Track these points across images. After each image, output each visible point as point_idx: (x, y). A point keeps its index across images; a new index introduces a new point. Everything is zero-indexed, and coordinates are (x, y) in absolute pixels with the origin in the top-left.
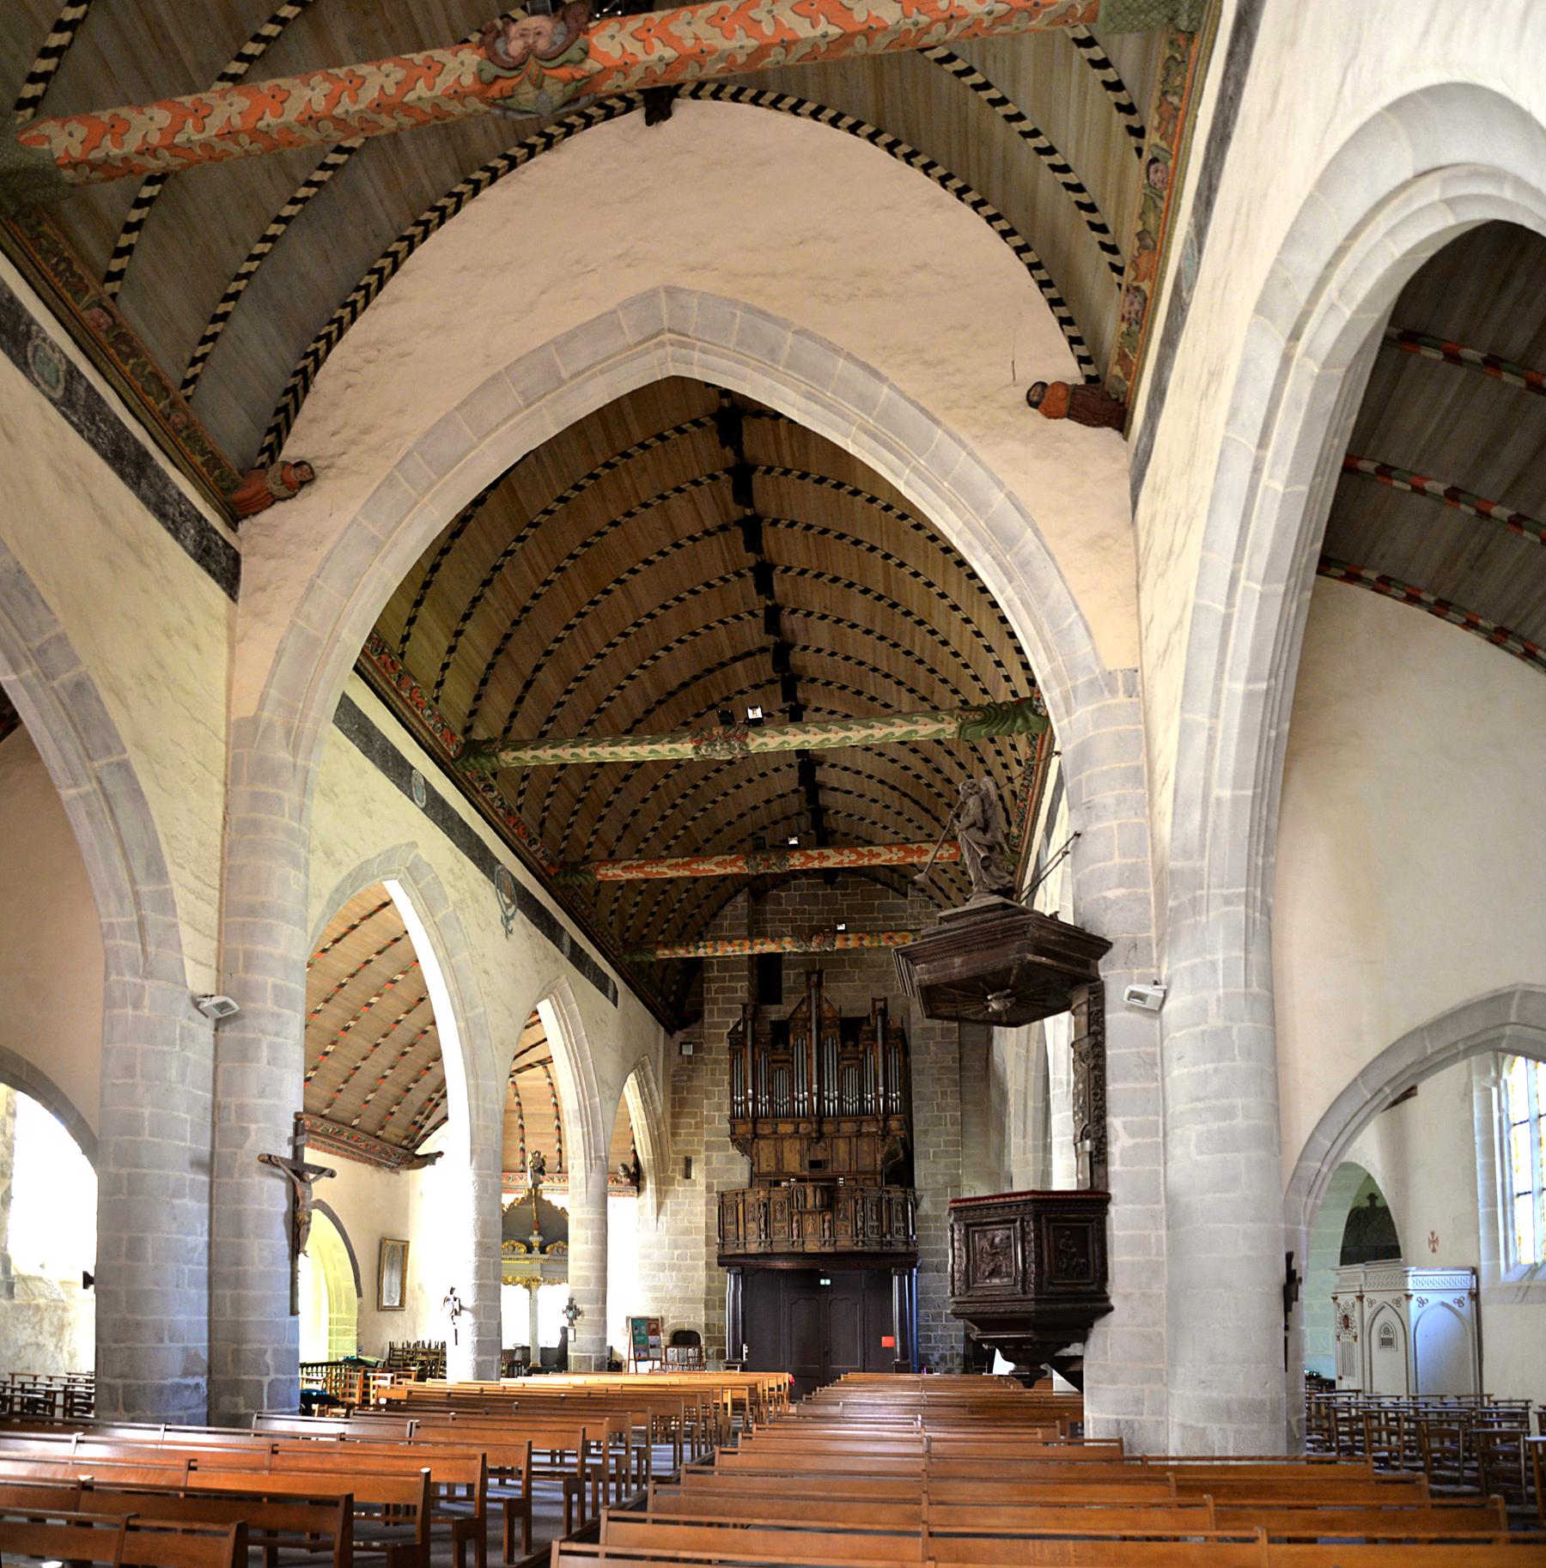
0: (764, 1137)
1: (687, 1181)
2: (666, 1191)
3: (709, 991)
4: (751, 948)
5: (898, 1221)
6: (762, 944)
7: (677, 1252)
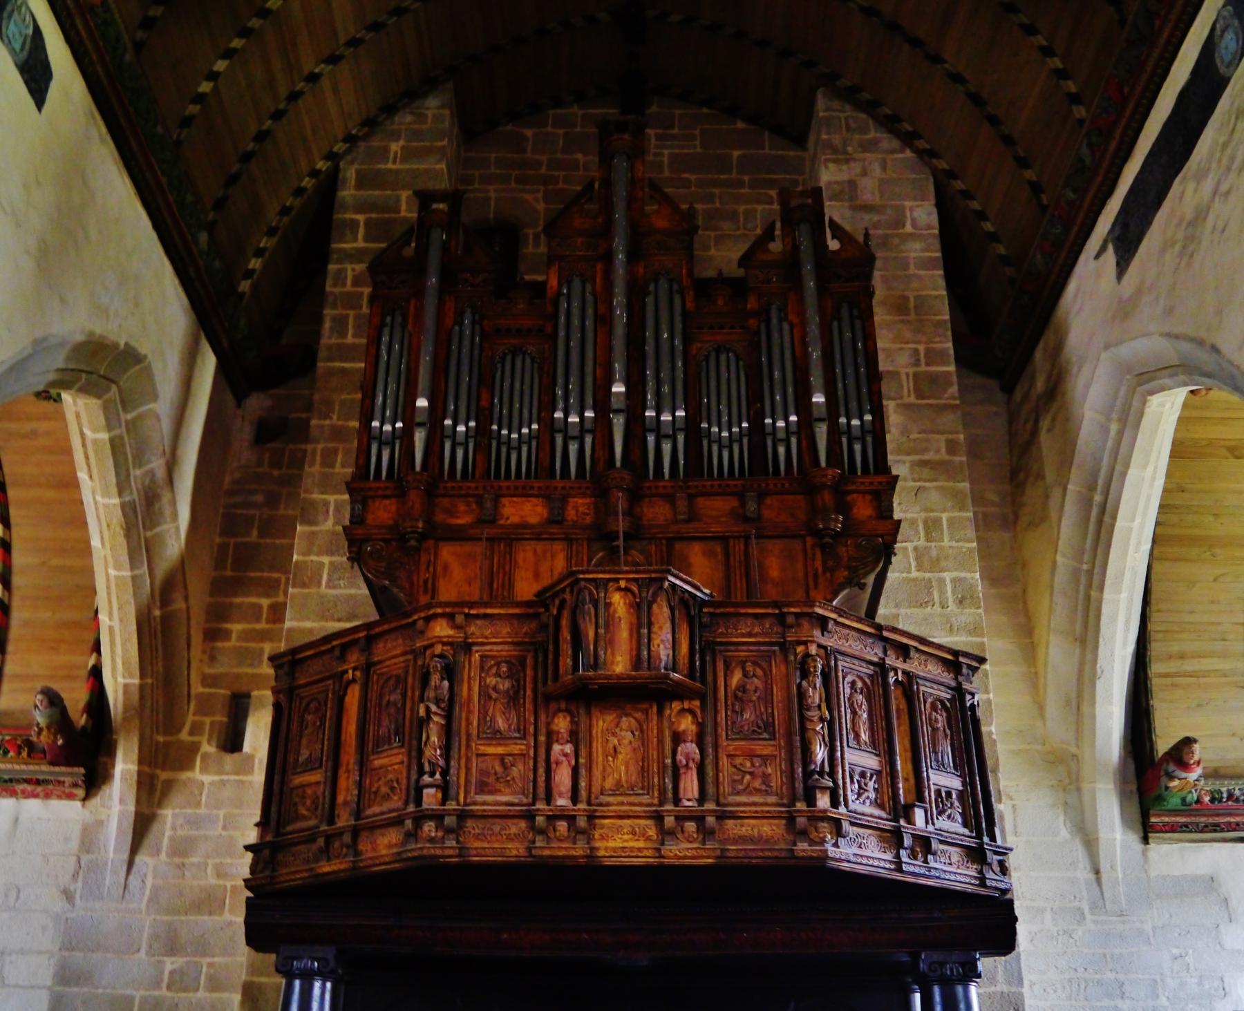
0: (457, 535)
1: (229, 759)
2: (169, 786)
5: (941, 766)
7: (170, 964)
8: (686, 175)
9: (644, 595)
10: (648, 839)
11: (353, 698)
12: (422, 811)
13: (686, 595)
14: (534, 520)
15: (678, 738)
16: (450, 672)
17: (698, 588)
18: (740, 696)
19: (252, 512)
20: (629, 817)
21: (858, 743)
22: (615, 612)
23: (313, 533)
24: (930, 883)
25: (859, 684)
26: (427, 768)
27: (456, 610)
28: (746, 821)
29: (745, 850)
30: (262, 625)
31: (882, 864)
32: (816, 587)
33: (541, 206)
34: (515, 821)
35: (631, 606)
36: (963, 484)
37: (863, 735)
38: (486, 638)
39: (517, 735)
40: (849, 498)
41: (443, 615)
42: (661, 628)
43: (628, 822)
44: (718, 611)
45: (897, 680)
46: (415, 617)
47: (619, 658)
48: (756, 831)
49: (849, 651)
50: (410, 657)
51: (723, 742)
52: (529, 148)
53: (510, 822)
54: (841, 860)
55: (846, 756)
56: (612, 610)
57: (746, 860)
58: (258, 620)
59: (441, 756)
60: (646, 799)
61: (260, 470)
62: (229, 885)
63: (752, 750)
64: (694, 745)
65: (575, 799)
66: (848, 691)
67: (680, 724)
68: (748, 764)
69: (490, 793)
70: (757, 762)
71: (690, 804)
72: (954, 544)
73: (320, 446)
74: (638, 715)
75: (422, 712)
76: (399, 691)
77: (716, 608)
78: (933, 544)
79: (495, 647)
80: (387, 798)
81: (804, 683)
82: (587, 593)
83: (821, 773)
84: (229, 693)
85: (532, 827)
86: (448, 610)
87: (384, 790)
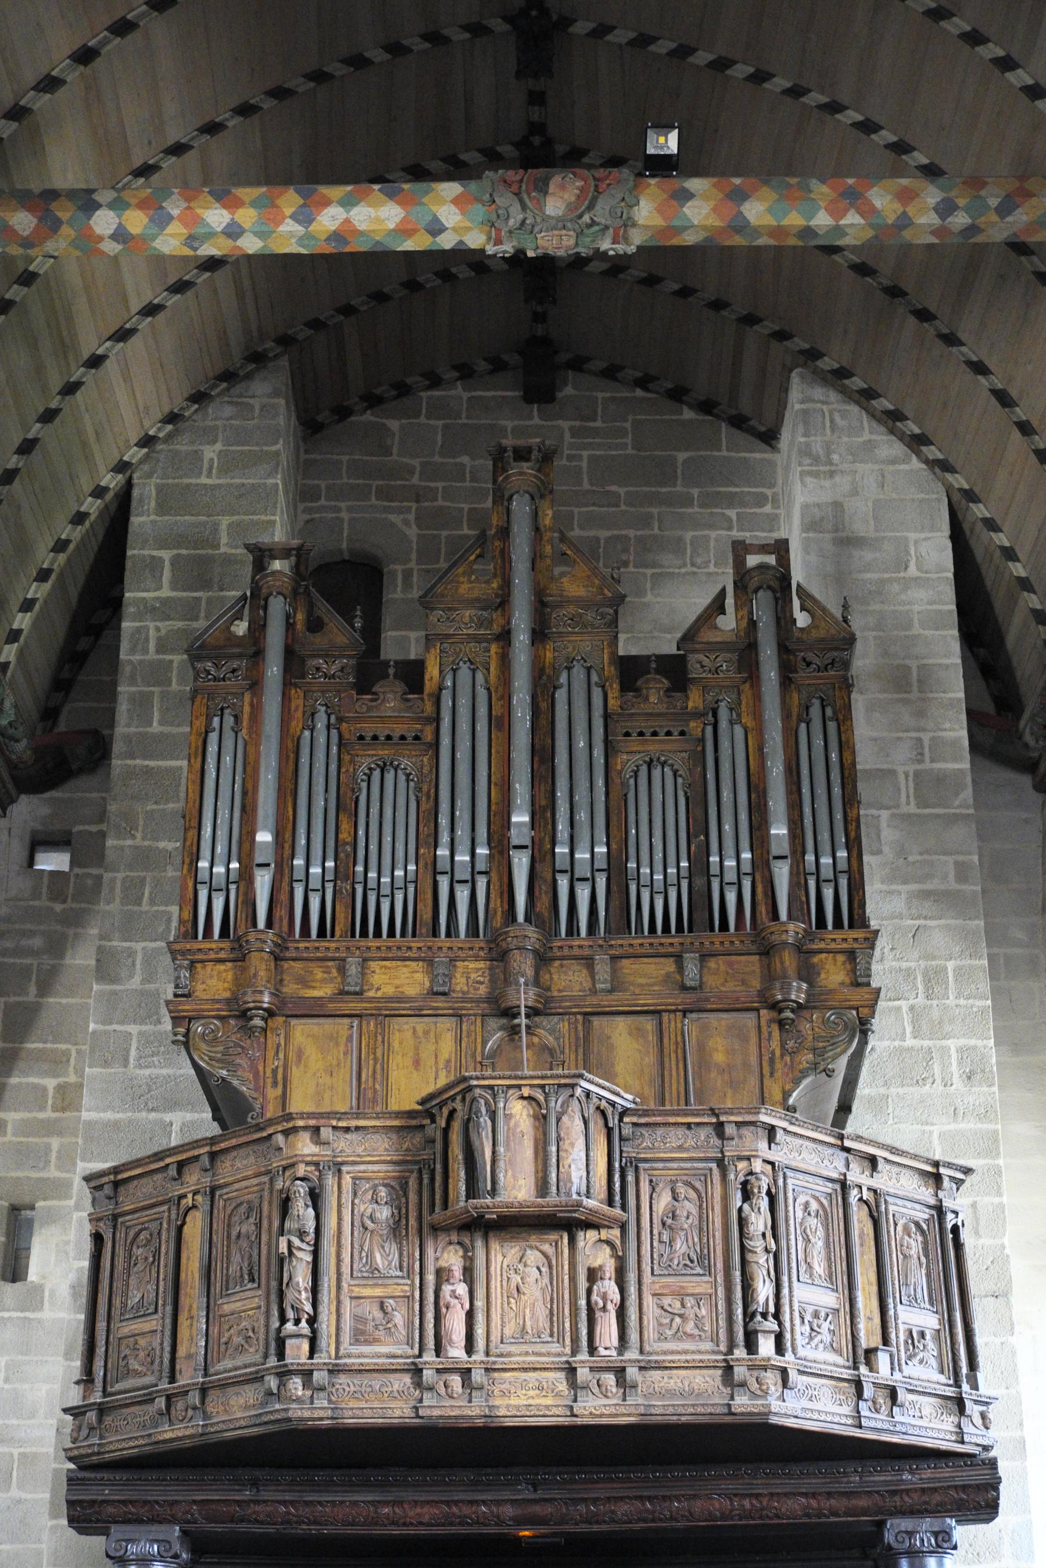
0: (314, 1011)
3: (140, 639)
4: (304, 217)
6: (347, 203)
8: (613, 488)
9: (553, 1104)
10: (558, 1395)
11: (195, 1228)
12: (286, 1365)
13: (604, 1103)
14: (411, 991)
15: (593, 1275)
16: (315, 1198)
17: (618, 1095)
18: (670, 1222)
19: (28, 961)
20: (535, 1369)
21: (811, 1276)
22: (516, 1125)
23: (115, 993)
24: (895, 1439)
25: (814, 1206)
26: (290, 1314)
27: (322, 1122)
28: (675, 1372)
29: (673, 1405)
30: (48, 1114)
31: (837, 1419)
32: (772, 1074)
33: (413, 532)
34: (398, 1375)
35: (536, 1117)
36: (976, 922)
37: (816, 1266)
38: (359, 1156)
39: (399, 1274)
40: (815, 959)
41: (305, 1128)
42: (572, 1145)
43: (531, 1374)
44: (643, 1120)
45: (861, 1199)
46: (270, 1131)
47: (522, 1182)
48: (686, 1383)
49: (803, 1166)
50: (265, 1179)
51: (647, 1278)
52: (395, 451)
53: (392, 1377)
54: (788, 1416)
55: (795, 1293)
56: (512, 1123)
57: (675, 1418)
58: (42, 1108)
59: (307, 1299)
60: (555, 1348)
61: (36, 903)
62: (16, 1452)
63: (682, 1287)
64: (613, 1283)
65: (470, 1348)
66: (800, 1214)
67: (596, 1257)
68: (678, 1304)
69: (367, 1342)
70: (690, 1302)
71: (607, 1353)
72: (962, 1002)
73: (120, 875)
74: (546, 1248)
75: (283, 1248)
76: (252, 1220)
77: (640, 1116)
78: (935, 1002)
79: (370, 1167)
80: (241, 1349)
81: (746, 1207)
82: (482, 1102)
83: (764, 1315)
84: (6, 1204)
85: (418, 1384)
86: (312, 1122)
87: (237, 1340)
